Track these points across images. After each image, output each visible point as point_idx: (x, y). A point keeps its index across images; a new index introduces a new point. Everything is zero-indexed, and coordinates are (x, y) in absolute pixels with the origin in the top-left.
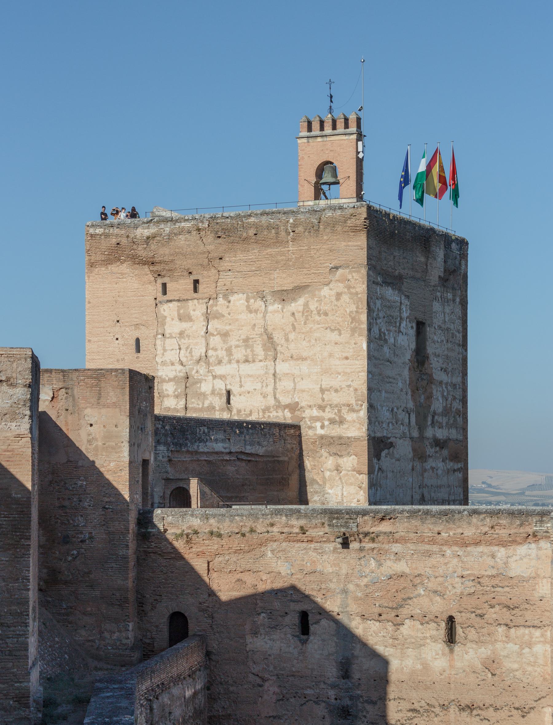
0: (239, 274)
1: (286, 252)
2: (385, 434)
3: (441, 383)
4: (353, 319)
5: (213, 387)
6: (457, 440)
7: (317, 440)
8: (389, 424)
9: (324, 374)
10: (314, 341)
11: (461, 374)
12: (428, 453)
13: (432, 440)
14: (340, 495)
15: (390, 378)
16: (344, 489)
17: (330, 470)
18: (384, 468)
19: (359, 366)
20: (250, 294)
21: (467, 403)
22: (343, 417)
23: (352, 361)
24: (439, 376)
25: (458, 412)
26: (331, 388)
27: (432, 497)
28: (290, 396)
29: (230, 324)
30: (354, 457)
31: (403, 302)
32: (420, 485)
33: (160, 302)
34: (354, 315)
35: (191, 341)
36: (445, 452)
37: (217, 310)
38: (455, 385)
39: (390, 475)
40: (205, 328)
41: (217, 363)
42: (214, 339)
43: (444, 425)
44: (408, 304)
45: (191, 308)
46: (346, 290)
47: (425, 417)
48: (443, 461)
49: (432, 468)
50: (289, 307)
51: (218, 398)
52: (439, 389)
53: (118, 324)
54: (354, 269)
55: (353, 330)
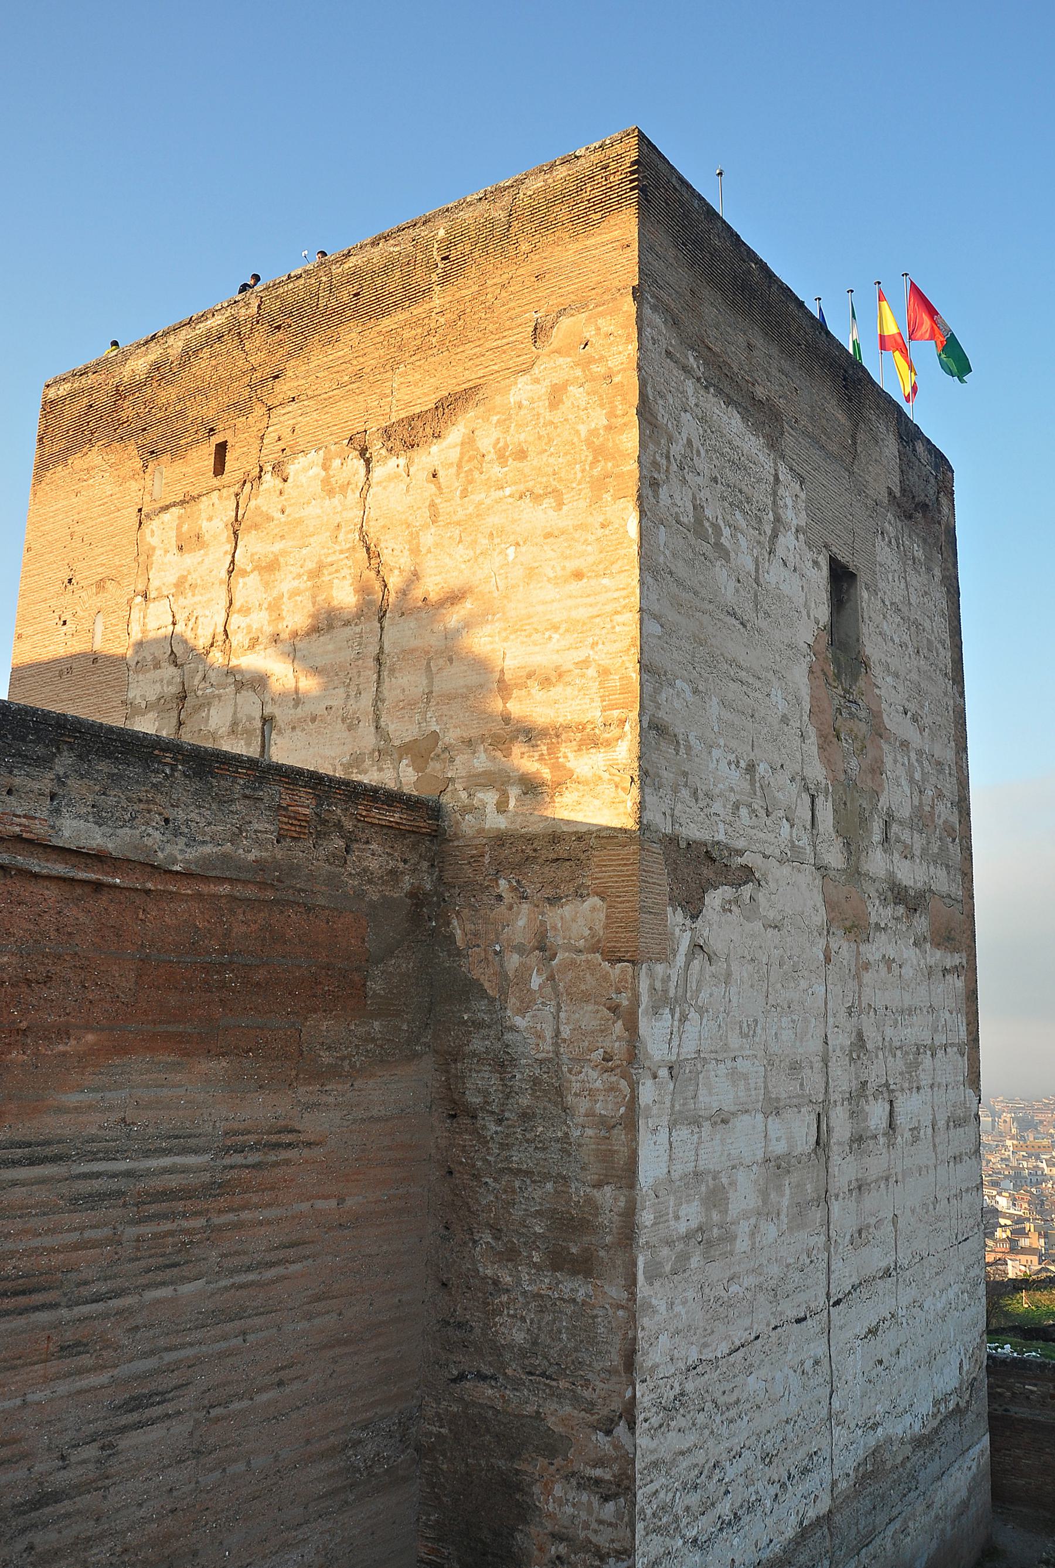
0: (312, 402)
1: (424, 315)
2: (721, 837)
3: (905, 744)
4: (599, 452)
5: (235, 713)
6: (949, 896)
7: (487, 848)
8: (736, 806)
9: (512, 637)
10: (485, 541)
11: (953, 744)
12: (873, 919)
13: (885, 886)
14: (549, 1034)
15: (740, 667)
16: (562, 1015)
17: (520, 949)
18: (717, 945)
19: (617, 595)
20: (333, 447)
21: (969, 814)
22: (564, 767)
23: (593, 582)
24: (896, 723)
25: (949, 830)
26: (529, 676)
27: (887, 1039)
28: (417, 717)
29: (282, 537)
30: (595, 900)
31: (781, 477)
32: (852, 1006)
33: (147, 516)
34: (601, 439)
35: (198, 598)
36: (921, 923)
37: (257, 508)
38: (939, 763)
39: (741, 972)
40: (229, 558)
41: (246, 644)
42: (245, 584)
43: (918, 853)
44: (803, 495)
45: (204, 515)
46: (578, 372)
47: (864, 821)
48: (915, 944)
49: (888, 962)
50: (423, 458)
51: (242, 742)
52: (899, 758)
53: (70, 587)
54: (600, 309)
55: (599, 485)
